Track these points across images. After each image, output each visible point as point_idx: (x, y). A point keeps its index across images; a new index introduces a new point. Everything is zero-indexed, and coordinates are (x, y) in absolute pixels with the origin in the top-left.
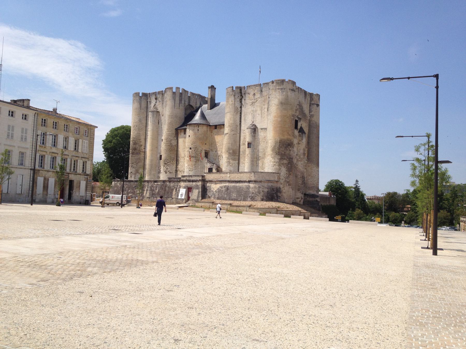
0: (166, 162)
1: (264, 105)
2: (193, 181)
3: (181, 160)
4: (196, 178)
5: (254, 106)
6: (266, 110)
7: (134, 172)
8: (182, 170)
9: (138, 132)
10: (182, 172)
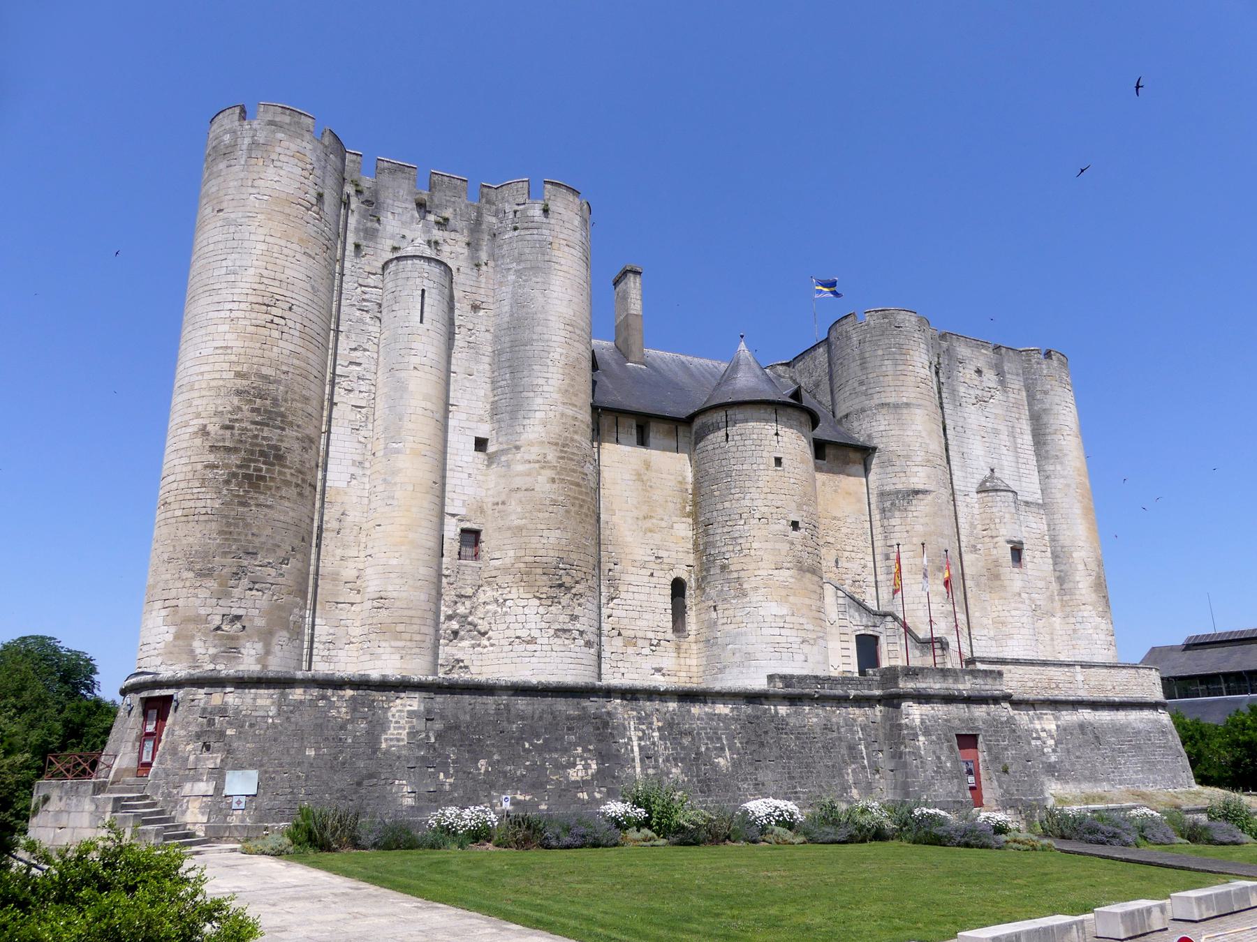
0: (566, 579)
1: (1018, 419)
2: (970, 700)
3: (628, 578)
4: (979, 681)
5: (987, 414)
6: (1027, 439)
7: (260, 622)
8: (640, 634)
9: (299, 350)
10: (640, 643)
